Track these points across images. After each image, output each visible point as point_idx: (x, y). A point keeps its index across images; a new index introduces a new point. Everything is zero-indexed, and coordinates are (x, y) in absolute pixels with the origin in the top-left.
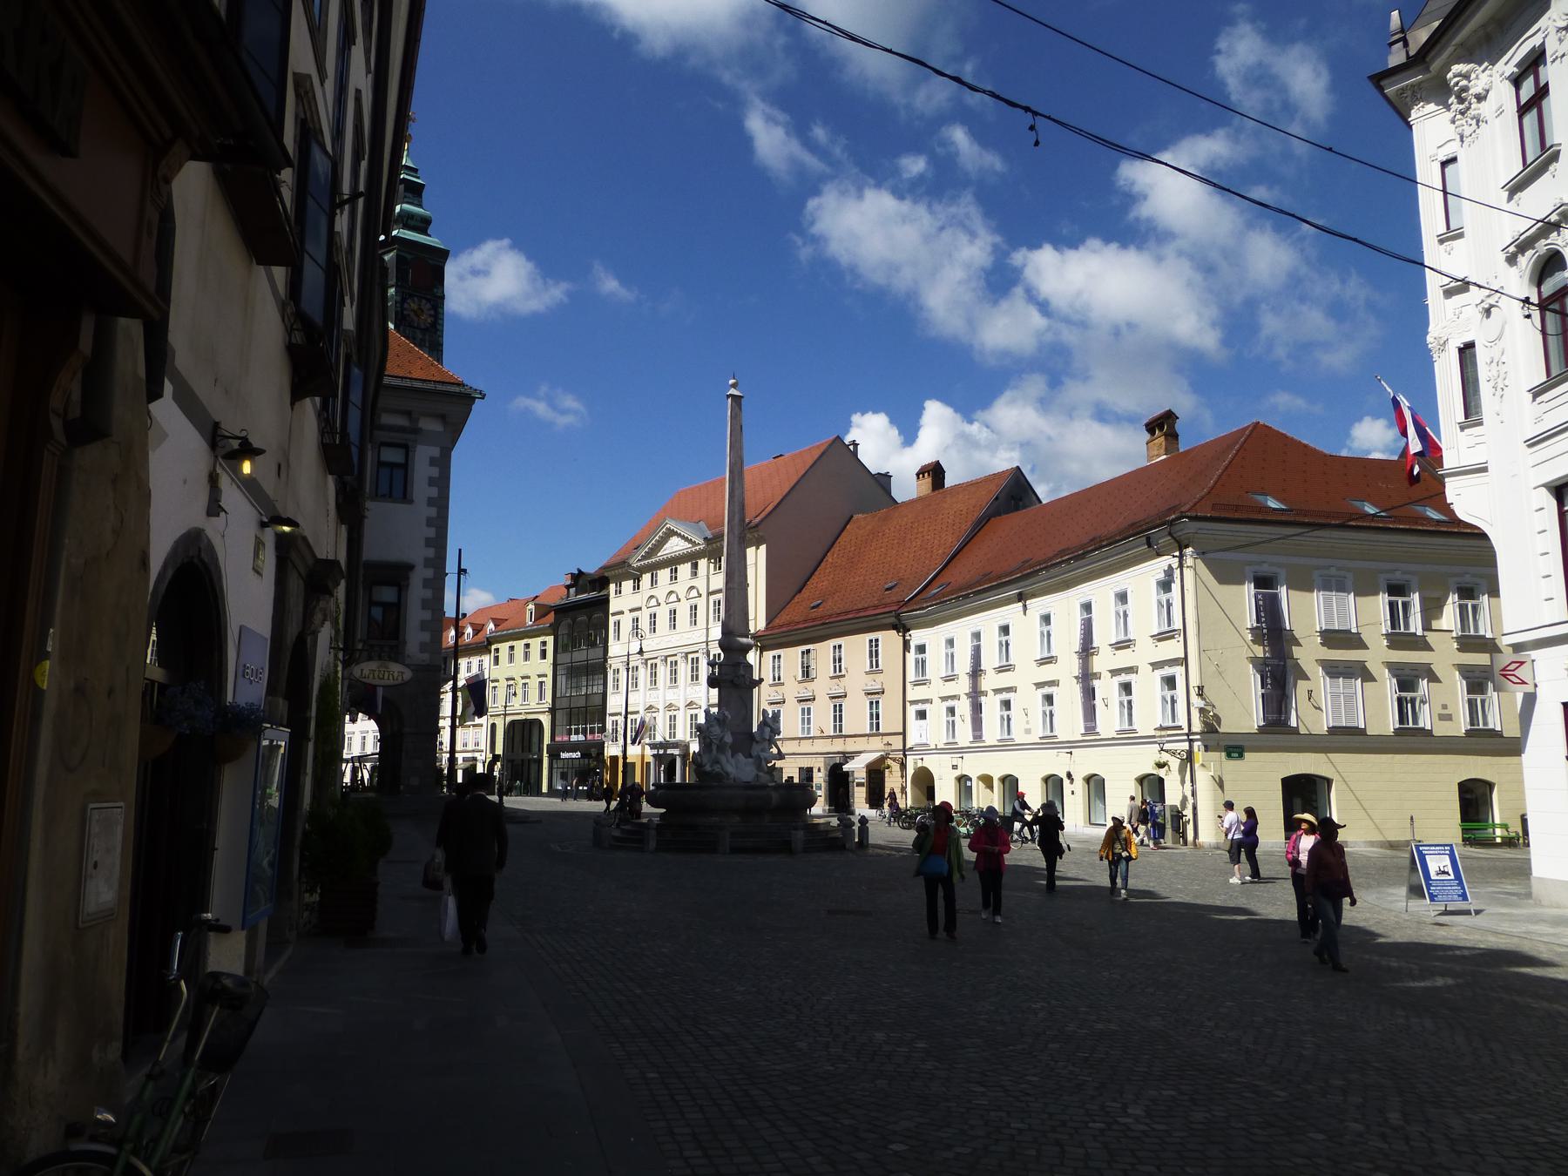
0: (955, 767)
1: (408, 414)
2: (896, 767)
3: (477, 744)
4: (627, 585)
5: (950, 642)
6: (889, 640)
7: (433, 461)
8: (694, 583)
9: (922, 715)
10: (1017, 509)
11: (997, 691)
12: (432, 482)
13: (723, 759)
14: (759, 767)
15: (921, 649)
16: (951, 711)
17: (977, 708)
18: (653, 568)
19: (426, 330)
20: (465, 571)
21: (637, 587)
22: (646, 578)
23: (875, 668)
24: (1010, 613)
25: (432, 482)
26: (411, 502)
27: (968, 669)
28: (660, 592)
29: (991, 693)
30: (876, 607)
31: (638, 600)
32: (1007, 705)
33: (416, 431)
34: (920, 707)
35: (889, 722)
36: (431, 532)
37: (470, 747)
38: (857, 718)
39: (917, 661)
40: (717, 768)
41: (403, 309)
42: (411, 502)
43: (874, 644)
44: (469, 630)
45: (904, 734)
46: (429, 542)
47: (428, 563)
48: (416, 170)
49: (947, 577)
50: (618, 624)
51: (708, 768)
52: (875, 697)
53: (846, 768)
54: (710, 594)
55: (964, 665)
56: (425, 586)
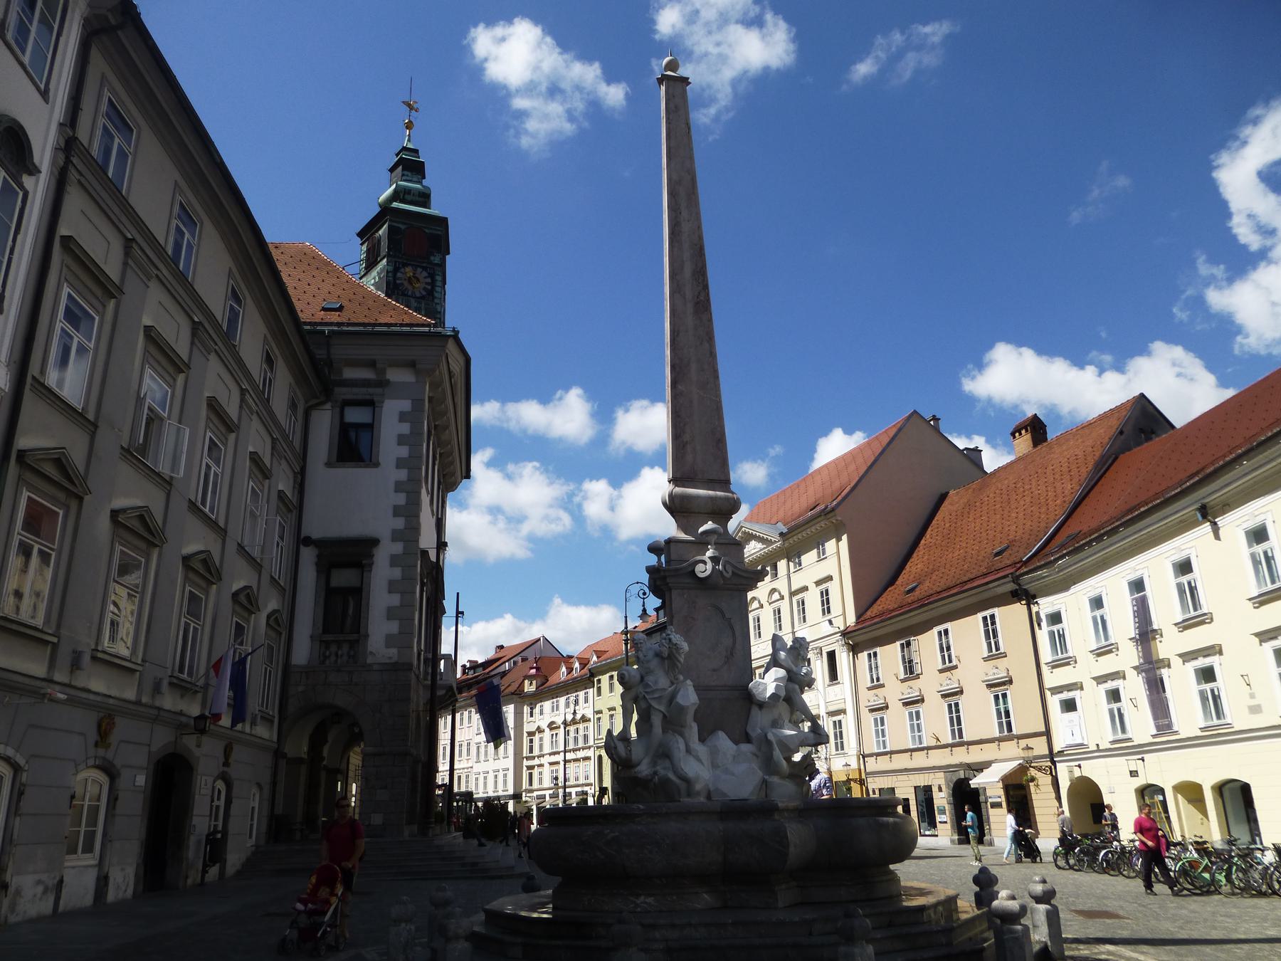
0: (1134, 774)
1: (372, 364)
2: (1044, 780)
3: (587, 778)
5: (1097, 603)
6: (1011, 617)
7: (403, 417)
8: (775, 585)
9: (1070, 706)
10: (1148, 439)
11: (1187, 657)
12: (401, 440)
14: (769, 765)
15: (1055, 618)
16: (1114, 696)
17: (1156, 687)
19: (423, 297)
23: (995, 653)
24: (1195, 542)
25: (401, 440)
26: (377, 465)
27: (1132, 631)
29: (1176, 662)
30: (985, 575)
32: (1207, 675)
33: (383, 383)
34: (1066, 695)
35: (1025, 718)
36: (401, 499)
37: (582, 781)
38: (980, 717)
39: (1052, 634)
40: (663, 770)
42: (377, 465)
43: (990, 622)
44: (577, 665)
45: (1047, 733)
46: (397, 511)
47: (396, 536)
48: (416, 151)
49: (1072, 528)
51: (644, 769)
52: (999, 687)
53: (974, 783)
54: (792, 594)
55: (1123, 625)
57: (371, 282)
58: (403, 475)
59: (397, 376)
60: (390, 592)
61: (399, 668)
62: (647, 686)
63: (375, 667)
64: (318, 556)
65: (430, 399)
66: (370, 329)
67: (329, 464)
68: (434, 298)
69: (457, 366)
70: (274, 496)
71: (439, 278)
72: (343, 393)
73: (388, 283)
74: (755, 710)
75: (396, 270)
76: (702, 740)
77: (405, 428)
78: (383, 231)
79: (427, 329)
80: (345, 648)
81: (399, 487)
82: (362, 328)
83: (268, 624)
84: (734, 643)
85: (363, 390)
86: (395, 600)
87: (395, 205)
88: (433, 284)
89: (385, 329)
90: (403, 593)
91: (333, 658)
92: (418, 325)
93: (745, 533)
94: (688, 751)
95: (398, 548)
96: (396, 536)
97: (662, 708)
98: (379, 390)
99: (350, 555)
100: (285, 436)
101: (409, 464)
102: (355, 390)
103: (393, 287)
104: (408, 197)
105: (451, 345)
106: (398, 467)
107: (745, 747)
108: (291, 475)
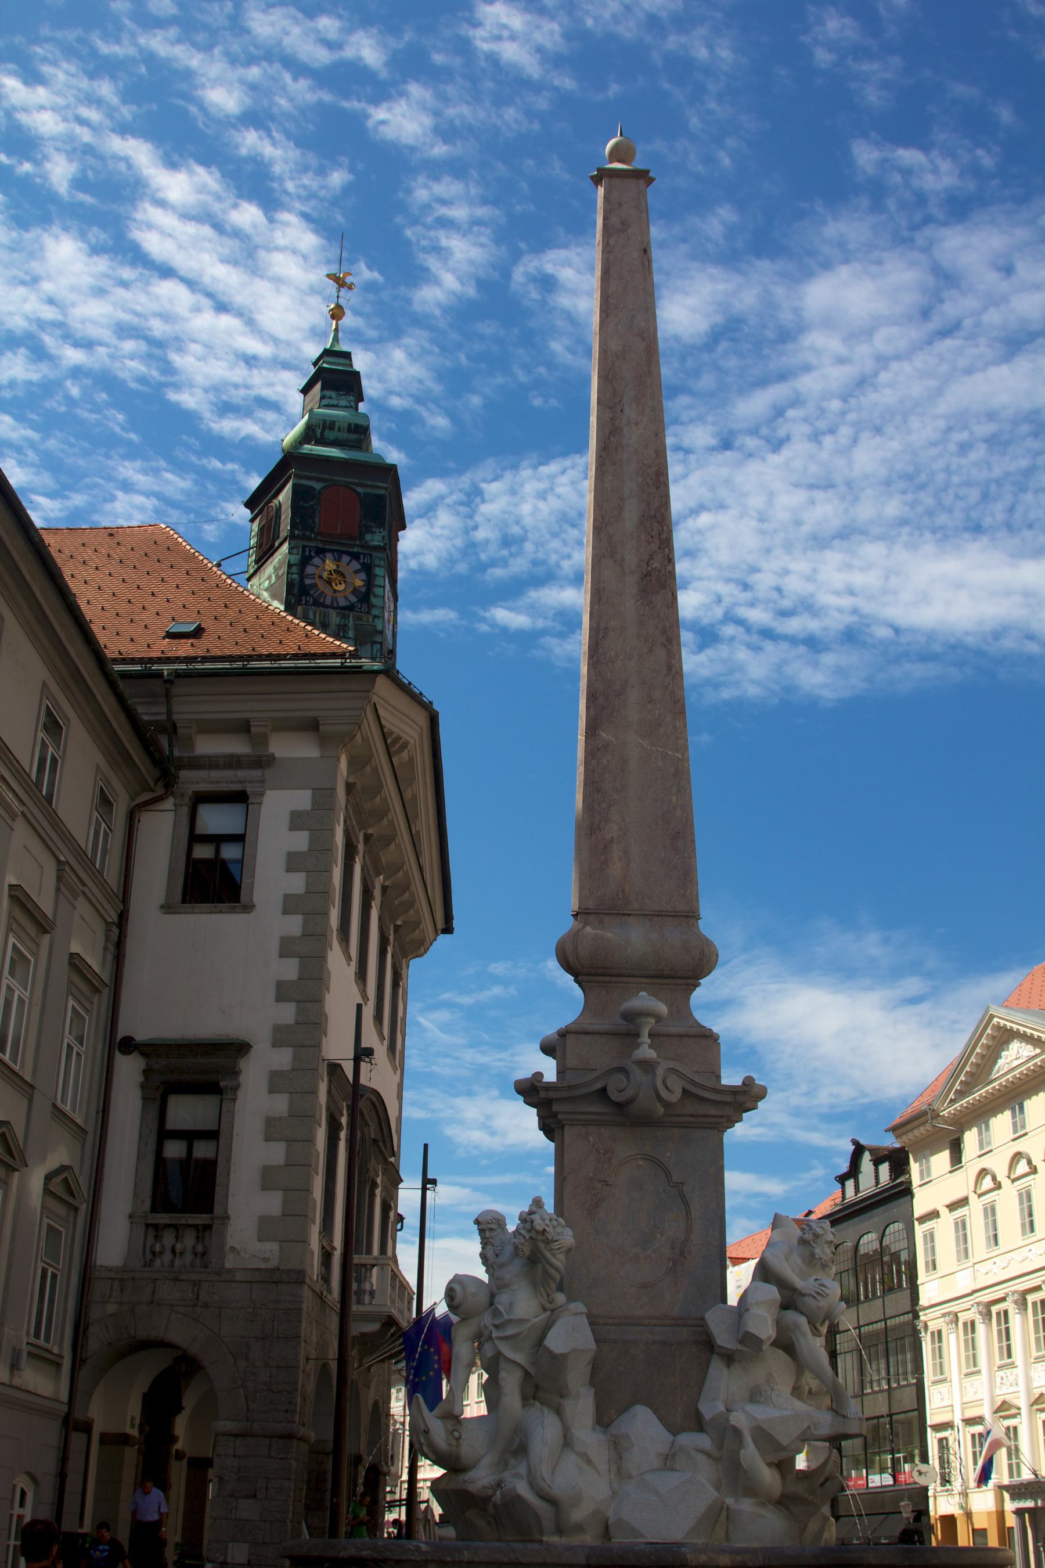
4: (941, 1160)
12: (294, 862)
13: (545, 1429)
14: (735, 1476)
18: (980, 1115)
19: (351, 608)
20: (369, 1052)
21: (956, 1158)
22: (970, 1138)
25: (294, 862)
26: (249, 908)
28: (998, 1163)
31: (961, 1184)
41: (302, 575)
42: (249, 908)
46: (283, 992)
47: (281, 1037)
50: (930, 1237)
56: (272, 1090)
57: (265, 588)
58: (294, 925)
59: (286, 748)
60: (267, 1139)
61: (284, 1278)
62: (497, 1313)
63: (239, 1276)
64: (146, 1072)
65: (350, 787)
66: (239, 664)
67: (167, 908)
68: (371, 606)
69: (409, 728)
70: (61, 964)
71: (379, 571)
72: (193, 780)
73: (290, 585)
74: (717, 1369)
75: (305, 561)
76: (603, 1421)
77: (301, 841)
78: (285, 497)
79: (337, 662)
80: (189, 1239)
81: (287, 947)
82: (227, 665)
83: (47, 1191)
84: (689, 1230)
85: (228, 774)
86: (276, 1153)
87: (308, 448)
88: (370, 583)
89: (266, 664)
90: (290, 1141)
91: (167, 1257)
92: (324, 656)
93: (998, 1028)
94: (567, 1442)
95: (283, 1059)
96: (281, 1037)
97: (519, 1357)
98: (257, 773)
99: (199, 1069)
100: (87, 862)
101: (306, 905)
102: (215, 774)
103: (299, 594)
104: (331, 435)
105: (382, 686)
106: (285, 912)
107: (689, 1439)
108: (100, 929)
